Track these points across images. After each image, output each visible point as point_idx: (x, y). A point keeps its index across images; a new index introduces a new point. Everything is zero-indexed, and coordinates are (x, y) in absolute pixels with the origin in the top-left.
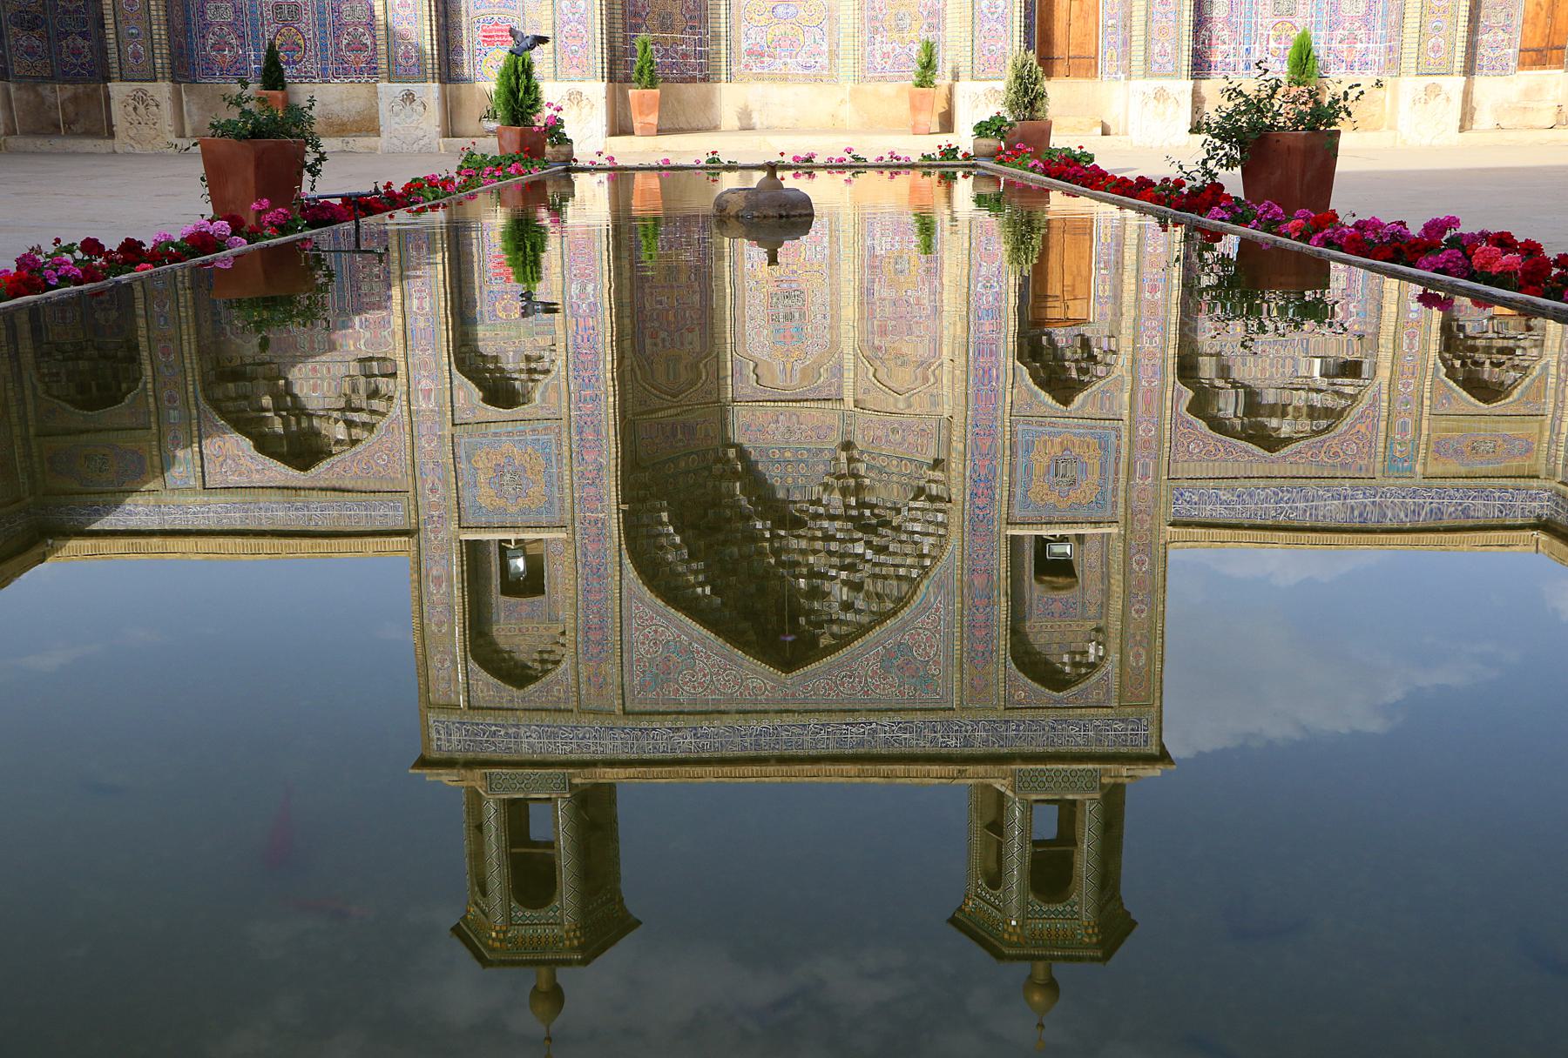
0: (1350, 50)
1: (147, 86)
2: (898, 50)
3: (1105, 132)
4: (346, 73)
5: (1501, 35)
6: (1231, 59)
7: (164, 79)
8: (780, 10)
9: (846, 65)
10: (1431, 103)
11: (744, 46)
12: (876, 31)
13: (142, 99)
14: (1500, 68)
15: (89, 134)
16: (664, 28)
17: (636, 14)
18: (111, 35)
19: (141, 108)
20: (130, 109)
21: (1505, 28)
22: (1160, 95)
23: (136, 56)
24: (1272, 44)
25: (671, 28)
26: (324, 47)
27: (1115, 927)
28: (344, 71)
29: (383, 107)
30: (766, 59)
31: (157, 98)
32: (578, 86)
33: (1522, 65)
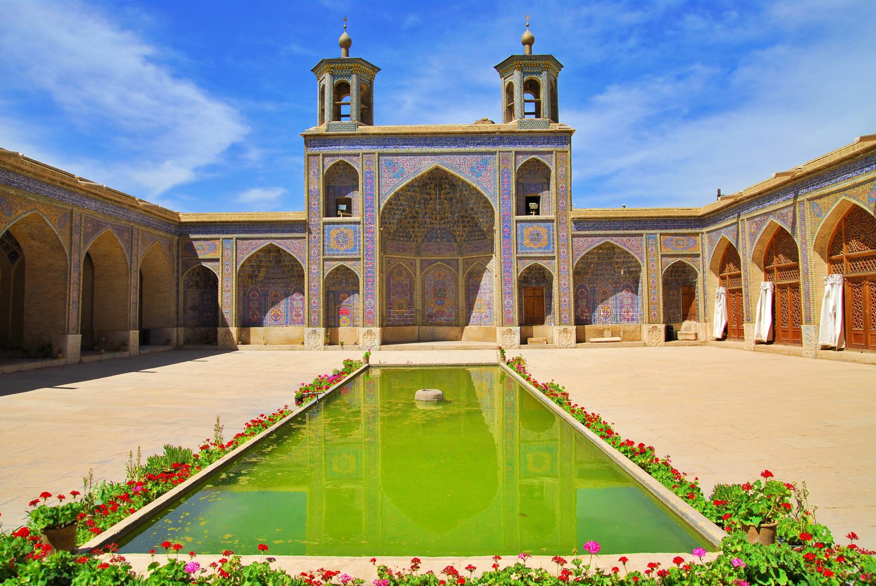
15: (209, 343)
17: (390, 304)
21: (677, 308)
22: (565, 331)
25: (402, 308)
26: (287, 315)
28: (294, 322)
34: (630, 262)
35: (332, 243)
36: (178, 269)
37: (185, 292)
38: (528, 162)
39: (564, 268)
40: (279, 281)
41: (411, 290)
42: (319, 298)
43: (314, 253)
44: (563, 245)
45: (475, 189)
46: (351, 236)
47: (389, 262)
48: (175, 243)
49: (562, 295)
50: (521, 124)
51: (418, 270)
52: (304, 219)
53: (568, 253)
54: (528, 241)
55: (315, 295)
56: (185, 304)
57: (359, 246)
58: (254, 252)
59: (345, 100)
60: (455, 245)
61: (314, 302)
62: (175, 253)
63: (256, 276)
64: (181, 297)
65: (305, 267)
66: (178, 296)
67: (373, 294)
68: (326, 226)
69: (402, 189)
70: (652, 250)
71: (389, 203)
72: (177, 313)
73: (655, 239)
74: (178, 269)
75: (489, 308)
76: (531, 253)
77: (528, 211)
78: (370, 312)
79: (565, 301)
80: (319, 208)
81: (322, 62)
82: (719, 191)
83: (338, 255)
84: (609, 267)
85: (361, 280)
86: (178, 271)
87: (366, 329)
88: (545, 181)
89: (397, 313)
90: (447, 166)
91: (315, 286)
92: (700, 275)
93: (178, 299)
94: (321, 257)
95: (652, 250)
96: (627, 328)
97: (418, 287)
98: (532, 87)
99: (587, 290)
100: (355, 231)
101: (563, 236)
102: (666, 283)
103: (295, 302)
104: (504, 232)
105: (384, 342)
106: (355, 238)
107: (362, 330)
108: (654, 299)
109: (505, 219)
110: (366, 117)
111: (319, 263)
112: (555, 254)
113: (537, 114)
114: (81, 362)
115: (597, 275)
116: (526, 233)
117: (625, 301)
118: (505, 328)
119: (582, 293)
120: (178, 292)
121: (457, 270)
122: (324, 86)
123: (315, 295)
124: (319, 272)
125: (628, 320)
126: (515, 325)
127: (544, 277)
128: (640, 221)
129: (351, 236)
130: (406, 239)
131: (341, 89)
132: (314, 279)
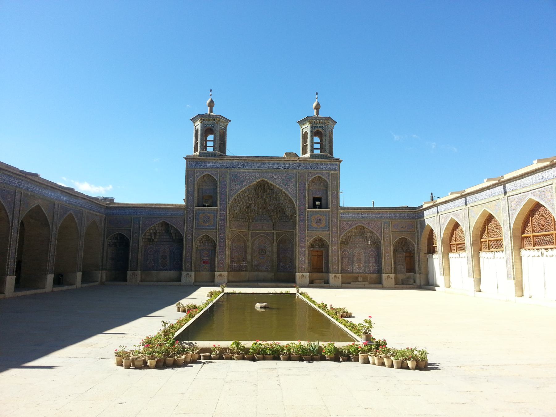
29: (183, 276)
33: (406, 272)
34: (374, 237)
36: (104, 235)
41: (245, 250)
45: (284, 193)
47: (232, 233)
48: (103, 219)
51: (250, 238)
59: (211, 137)
60: (272, 224)
62: (103, 224)
63: (153, 240)
64: (105, 252)
72: (102, 262)
74: (104, 235)
77: (315, 206)
79: (335, 259)
80: (193, 201)
82: (432, 194)
84: (361, 240)
87: (219, 273)
88: (324, 188)
92: (416, 246)
97: (249, 248)
99: (348, 252)
102: (395, 251)
114: (52, 291)
115: (354, 244)
117: (371, 259)
119: (345, 254)
120: (103, 249)
121: (273, 240)
127: (323, 244)
128: (379, 213)
130: (243, 220)
131: (207, 131)
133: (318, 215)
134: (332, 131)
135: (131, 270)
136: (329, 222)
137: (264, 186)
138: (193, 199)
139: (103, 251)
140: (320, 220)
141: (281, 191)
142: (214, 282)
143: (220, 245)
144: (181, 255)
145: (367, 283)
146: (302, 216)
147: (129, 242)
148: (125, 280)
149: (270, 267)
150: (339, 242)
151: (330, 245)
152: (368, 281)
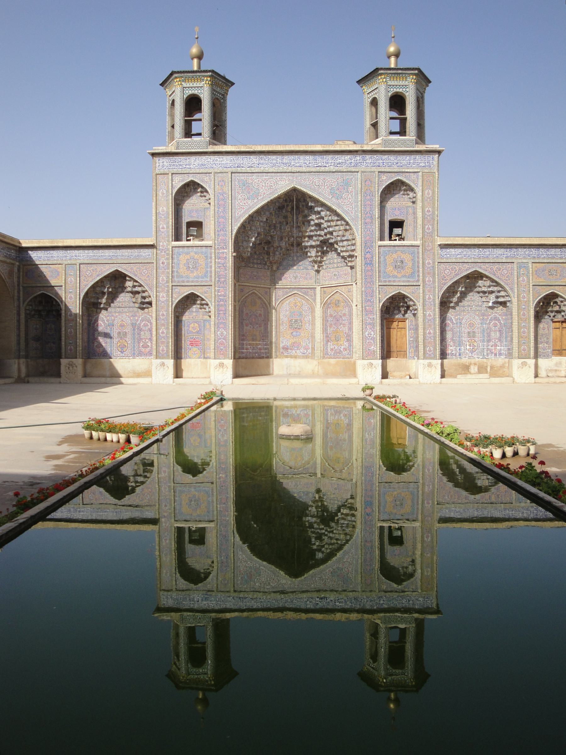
0: (495, 349)
1: (74, 360)
2: (336, 348)
3: (410, 378)
4: (141, 356)
5: (546, 345)
6: (454, 352)
7: (79, 358)
8: (294, 333)
9: (318, 353)
10: (524, 368)
11: (281, 346)
12: (328, 341)
13: (71, 365)
14: (547, 356)
15: (52, 376)
16: (253, 340)
17: (243, 335)
18: (63, 343)
19: (71, 368)
20: (67, 368)
21: (547, 343)
22: (430, 365)
23: (71, 350)
24: (468, 347)
25: (256, 340)
27: (421, 676)
28: (140, 354)
30: (289, 350)
31: (77, 364)
32: (223, 361)
34: (499, 292)
35: (182, 270)
36: (19, 297)
37: (26, 321)
38: (392, 183)
39: (429, 298)
40: (126, 310)
42: (168, 328)
43: (163, 280)
44: (429, 273)
46: (202, 262)
47: (242, 291)
48: (16, 269)
49: (427, 326)
50: (385, 142)
52: (152, 243)
53: (434, 282)
54: (392, 268)
55: (163, 325)
56: (27, 334)
57: (211, 272)
58: (98, 278)
61: (163, 333)
62: (15, 280)
65: (153, 294)
66: (19, 326)
67: (225, 324)
68: (176, 250)
69: (258, 212)
70: (523, 281)
71: (243, 227)
72: (19, 343)
73: (527, 268)
75: (348, 340)
76: (394, 281)
78: (222, 344)
79: (430, 333)
80: (168, 232)
81: (171, 74)
83: (188, 281)
85: (212, 308)
86: (19, 300)
87: (217, 361)
89: (250, 344)
90: (305, 187)
91: (163, 315)
93: (19, 329)
94: (170, 285)
95: (523, 281)
96: (494, 363)
98: (397, 102)
100: (206, 257)
101: (429, 263)
103: (142, 333)
104: (365, 258)
105: (237, 375)
106: (206, 264)
107: (214, 362)
108: (524, 332)
109: (367, 245)
110: (218, 132)
111: (168, 291)
112: (421, 283)
113: (402, 132)
116: (389, 260)
117: (493, 334)
118: (366, 362)
120: (19, 321)
121: (315, 300)
122: (173, 101)
123: (163, 325)
124: (168, 301)
125: (496, 355)
126: (376, 359)
129: (202, 262)
131: (193, 104)
132: (163, 308)
133: (399, 253)
134: (423, 97)
135: (66, 358)
136: (418, 267)
137: (298, 201)
138: (168, 227)
139: (19, 326)
140: (402, 262)
141: (329, 209)
142: (210, 378)
143: (219, 310)
144: (150, 330)
145: (487, 376)
146: (368, 255)
147: (61, 309)
148: (58, 375)
149: (310, 351)
150: (437, 302)
151: (420, 307)
152: (487, 372)
